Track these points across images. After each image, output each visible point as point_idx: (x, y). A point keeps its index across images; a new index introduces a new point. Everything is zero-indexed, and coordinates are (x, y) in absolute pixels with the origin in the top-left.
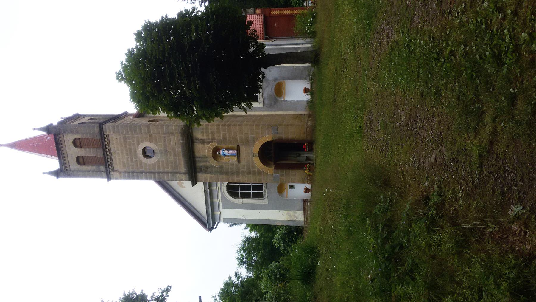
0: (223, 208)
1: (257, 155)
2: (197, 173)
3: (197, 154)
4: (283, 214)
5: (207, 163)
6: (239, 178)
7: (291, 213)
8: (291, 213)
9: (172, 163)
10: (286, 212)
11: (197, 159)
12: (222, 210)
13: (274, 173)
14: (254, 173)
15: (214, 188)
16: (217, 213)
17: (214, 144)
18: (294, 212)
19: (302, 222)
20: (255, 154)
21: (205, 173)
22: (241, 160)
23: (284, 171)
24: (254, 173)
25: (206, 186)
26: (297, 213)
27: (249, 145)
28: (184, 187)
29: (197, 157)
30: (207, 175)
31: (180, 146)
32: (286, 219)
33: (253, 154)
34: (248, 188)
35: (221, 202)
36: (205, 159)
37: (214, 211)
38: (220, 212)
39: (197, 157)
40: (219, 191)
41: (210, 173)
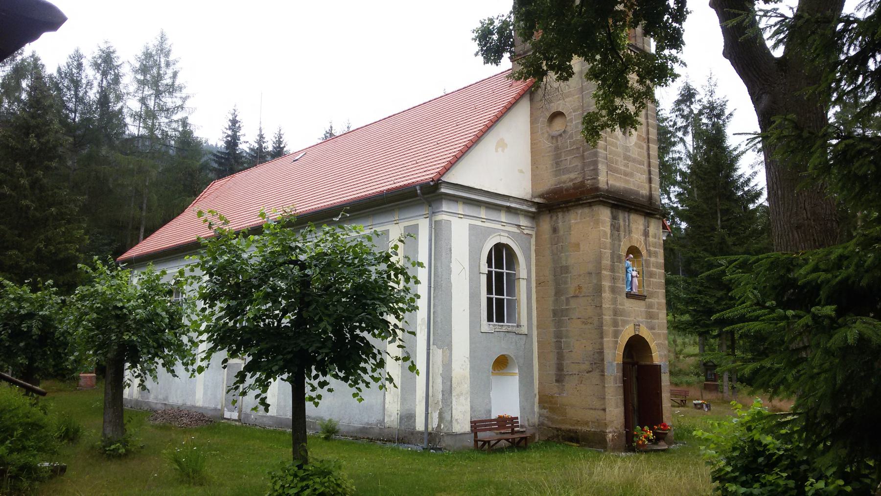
0: (472, 227)
1: (637, 333)
2: (609, 209)
3: (633, 217)
4: (462, 365)
6: (608, 292)
7: (466, 387)
8: (466, 386)
9: (616, 164)
10: (467, 372)
11: (626, 215)
12: (467, 222)
13: (618, 364)
14: (615, 324)
15: (503, 217)
16: (460, 209)
17: (644, 252)
18: (467, 393)
19: (450, 412)
20: (639, 329)
21: (612, 225)
22: (632, 300)
23: (620, 385)
24: (615, 324)
25: (516, 203)
26: (466, 399)
27: (646, 318)
28: (497, 151)
29: (629, 216)
30: (609, 227)
32: (454, 375)
33: (639, 325)
34: (500, 291)
35: (479, 223)
36: (627, 232)
37: (464, 203)
38: (462, 216)
39: (629, 216)
40: (499, 226)
41: (612, 235)
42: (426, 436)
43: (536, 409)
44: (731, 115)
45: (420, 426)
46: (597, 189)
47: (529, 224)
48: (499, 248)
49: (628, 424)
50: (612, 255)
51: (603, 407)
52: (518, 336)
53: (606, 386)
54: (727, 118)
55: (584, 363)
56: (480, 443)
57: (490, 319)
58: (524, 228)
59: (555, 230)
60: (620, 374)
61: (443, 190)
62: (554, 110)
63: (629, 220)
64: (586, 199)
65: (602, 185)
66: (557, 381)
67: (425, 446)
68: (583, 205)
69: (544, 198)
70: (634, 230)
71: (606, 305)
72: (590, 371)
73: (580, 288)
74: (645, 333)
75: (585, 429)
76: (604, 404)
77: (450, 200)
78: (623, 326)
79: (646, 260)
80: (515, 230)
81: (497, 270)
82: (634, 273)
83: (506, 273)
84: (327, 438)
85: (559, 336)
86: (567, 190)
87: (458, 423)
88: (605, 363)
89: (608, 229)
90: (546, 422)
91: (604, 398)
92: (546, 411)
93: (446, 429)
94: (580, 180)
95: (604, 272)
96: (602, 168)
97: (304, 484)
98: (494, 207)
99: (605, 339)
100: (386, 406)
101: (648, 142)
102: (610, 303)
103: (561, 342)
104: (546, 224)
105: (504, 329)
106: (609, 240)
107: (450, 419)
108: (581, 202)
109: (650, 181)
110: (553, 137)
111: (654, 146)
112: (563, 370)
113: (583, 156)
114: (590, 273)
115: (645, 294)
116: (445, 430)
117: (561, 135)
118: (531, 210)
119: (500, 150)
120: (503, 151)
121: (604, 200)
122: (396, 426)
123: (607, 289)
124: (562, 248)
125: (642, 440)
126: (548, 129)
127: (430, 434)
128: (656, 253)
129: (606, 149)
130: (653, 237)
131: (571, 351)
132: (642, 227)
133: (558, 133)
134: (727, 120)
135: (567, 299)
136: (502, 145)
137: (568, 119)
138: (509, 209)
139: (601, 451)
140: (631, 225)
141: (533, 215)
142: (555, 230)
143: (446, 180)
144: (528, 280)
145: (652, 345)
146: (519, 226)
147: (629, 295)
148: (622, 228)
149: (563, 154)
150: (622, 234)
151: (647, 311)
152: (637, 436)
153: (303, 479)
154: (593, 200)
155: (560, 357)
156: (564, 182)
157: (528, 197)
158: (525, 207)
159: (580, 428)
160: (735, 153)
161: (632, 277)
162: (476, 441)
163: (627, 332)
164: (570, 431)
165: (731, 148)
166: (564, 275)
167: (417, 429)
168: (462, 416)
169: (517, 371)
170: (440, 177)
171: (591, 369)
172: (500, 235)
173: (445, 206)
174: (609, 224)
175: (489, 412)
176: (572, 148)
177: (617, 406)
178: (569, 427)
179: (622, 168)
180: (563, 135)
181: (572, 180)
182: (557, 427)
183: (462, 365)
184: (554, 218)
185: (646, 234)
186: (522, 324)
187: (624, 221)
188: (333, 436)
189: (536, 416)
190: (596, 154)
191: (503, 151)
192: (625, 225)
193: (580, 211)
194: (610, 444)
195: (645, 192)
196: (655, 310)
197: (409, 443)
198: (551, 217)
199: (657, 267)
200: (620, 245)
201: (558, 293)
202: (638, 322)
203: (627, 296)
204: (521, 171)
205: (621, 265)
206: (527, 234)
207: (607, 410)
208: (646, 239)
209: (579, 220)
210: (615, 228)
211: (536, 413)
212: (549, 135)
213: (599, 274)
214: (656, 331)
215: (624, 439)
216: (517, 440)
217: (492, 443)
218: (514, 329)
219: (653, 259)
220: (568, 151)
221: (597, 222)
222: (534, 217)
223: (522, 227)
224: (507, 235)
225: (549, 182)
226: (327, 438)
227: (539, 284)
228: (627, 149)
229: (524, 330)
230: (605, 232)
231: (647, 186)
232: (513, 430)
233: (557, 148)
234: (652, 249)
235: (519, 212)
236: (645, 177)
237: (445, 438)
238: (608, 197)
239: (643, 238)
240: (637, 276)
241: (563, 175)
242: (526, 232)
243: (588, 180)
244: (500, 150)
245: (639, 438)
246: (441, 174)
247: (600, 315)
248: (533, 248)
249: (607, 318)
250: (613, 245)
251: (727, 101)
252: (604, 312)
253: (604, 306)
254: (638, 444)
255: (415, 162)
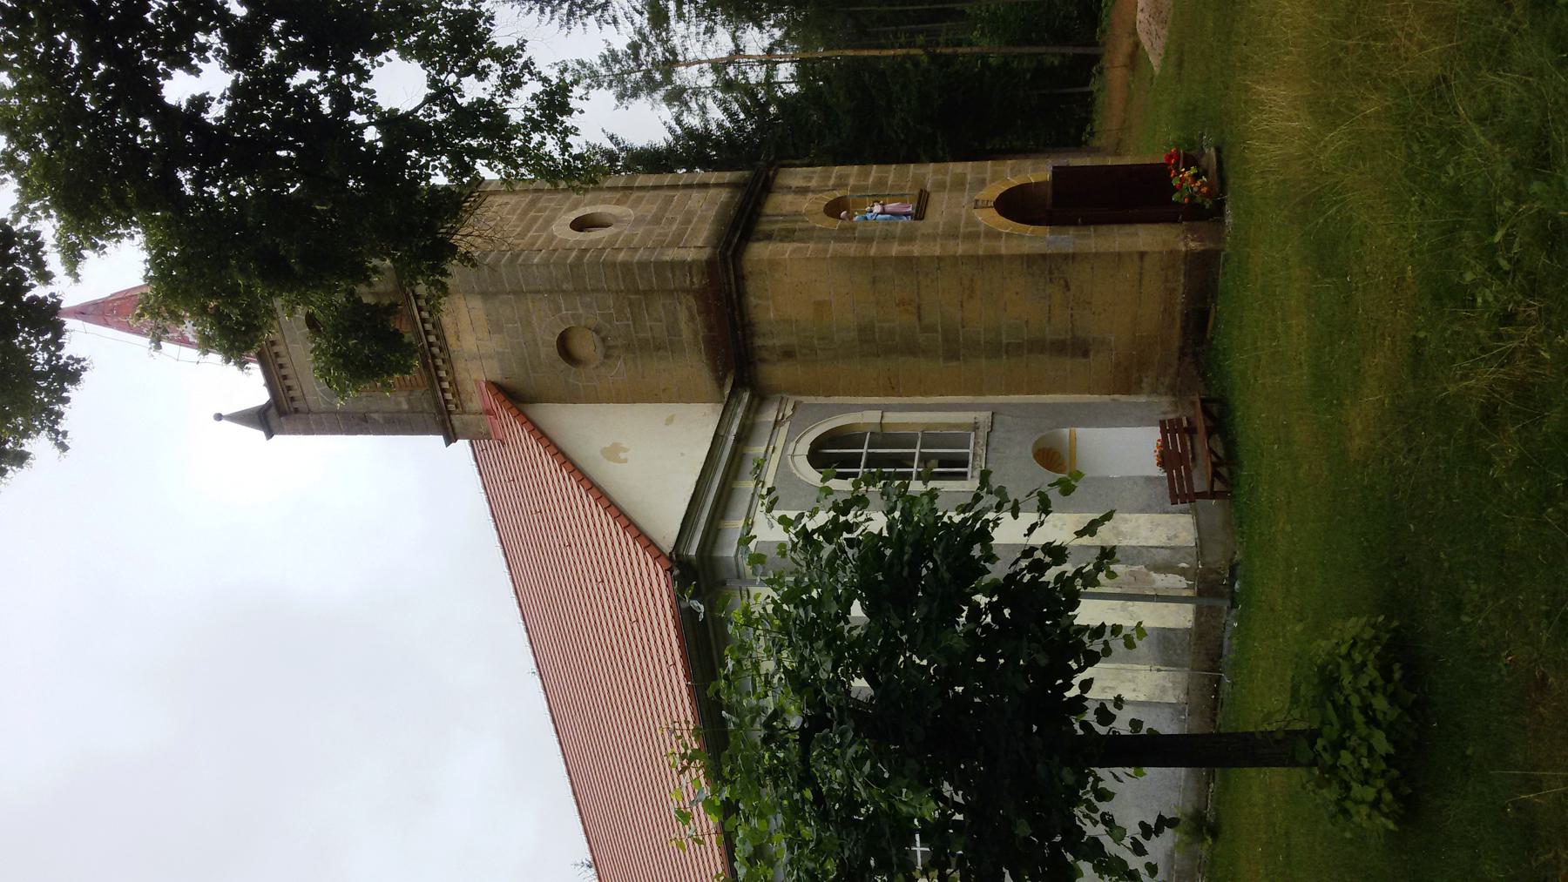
5: (800, 224)
6: (910, 247)
14: (973, 236)
17: (838, 194)
20: (983, 201)
22: (929, 211)
23: (1092, 229)
25: (730, 424)
26: (1126, 521)
27: (964, 190)
28: (625, 461)
30: (786, 245)
31: (716, 207)
33: (977, 201)
37: (723, 517)
40: (775, 459)
41: (801, 240)
42: (1205, 602)
43: (1142, 399)
44: (611, 138)
45: (1180, 617)
46: (710, 263)
47: (776, 406)
48: (817, 457)
49: (1171, 219)
50: (838, 239)
51: (1136, 258)
52: (996, 426)
53: (1094, 250)
54: (617, 144)
55: (1050, 296)
56: (1218, 486)
57: (963, 476)
58: (781, 415)
59: (788, 354)
60: (1072, 231)
61: (693, 552)
62: (554, 351)
63: (774, 216)
64: (729, 284)
65: (705, 254)
66: (1086, 354)
67: (1225, 604)
68: (741, 294)
69: (725, 376)
70: (794, 209)
71: (936, 250)
72: (1066, 282)
73: (902, 303)
74: (993, 192)
75: (1180, 297)
76: (1130, 254)
77: (714, 542)
78: (977, 224)
79: (852, 190)
80: (783, 431)
81: (862, 463)
82: (877, 208)
83: (869, 448)
84: (1214, 832)
85: (996, 349)
86: (710, 328)
87: (1176, 536)
88: (1050, 251)
89: (788, 248)
90: (1167, 381)
91: (1119, 254)
92: (1145, 380)
93: (1190, 559)
94: (692, 302)
95: (872, 252)
96: (670, 255)
97: (1358, 718)
98: (736, 460)
99: (1003, 251)
100: (1142, 698)
101: (631, 188)
102: (932, 244)
103: (1008, 344)
104: (775, 373)
105: (982, 452)
106: (811, 245)
107: (1168, 551)
108: (735, 296)
109: (704, 186)
110: (606, 356)
111: (638, 180)
112: (1063, 343)
113: (645, 292)
114: (874, 282)
115: (916, 192)
116: (1192, 560)
117: (604, 340)
118: (746, 400)
119: (622, 456)
120: (626, 450)
121: (731, 249)
122: (1186, 675)
123: (905, 248)
124: (823, 339)
125: (1200, 188)
126: (592, 366)
127: (1200, 594)
128: (840, 177)
129: (636, 249)
130: (810, 181)
131: (1027, 321)
132: (790, 197)
133: (600, 350)
134: (622, 146)
135: (925, 329)
136: (613, 453)
137: (573, 324)
138: (744, 437)
139: (1226, 256)
140: (784, 212)
141: (756, 401)
142: (788, 354)
143: (672, 545)
144: (886, 408)
145: (1015, 182)
146: (777, 423)
147: (919, 214)
148: (789, 226)
149: (641, 335)
150: (799, 225)
151: (950, 191)
152: (1192, 197)
153: (1348, 725)
154: (732, 272)
155: (1038, 346)
156: (696, 333)
157: (720, 408)
158: (740, 412)
159: (1179, 308)
160: (679, 131)
161: (883, 212)
162: (1213, 495)
163: (990, 218)
164: (1182, 328)
165: (670, 138)
166: (877, 336)
167: (1189, 625)
168: (1160, 528)
169: (1066, 431)
170: (665, 554)
171: (1062, 282)
172: (793, 456)
173: (729, 550)
174: (780, 245)
175: (1149, 480)
176: (629, 315)
177: (1137, 234)
178: (1176, 331)
179: (674, 227)
180: (602, 334)
181: (692, 318)
182: (1177, 355)
183: (1055, 526)
184: (764, 354)
185: (803, 191)
186: (973, 421)
187: (777, 222)
188: (1210, 819)
189: (1155, 399)
190: (643, 265)
191: (626, 450)
192: (783, 221)
193: (753, 300)
194: (1210, 245)
195: (724, 195)
196: (948, 178)
197: (1221, 646)
198: (763, 360)
199: (868, 175)
200: (821, 229)
201: (911, 349)
202: (969, 202)
203: (922, 219)
204: (670, 421)
205: (860, 228)
206: (794, 409)
207: (1143, 249)
208: (813, 191)
209: (770, 302)
210: (788, 235)
211: (1150, 399)
212: (602, 364)
213: (875, 262)
214: (988, 176)
215: (1197, 224)
216: (1209, 423)
217: (1214, 459)
218: (982, 433)
219: (852, 181)
220: (634, 324)
221: (774, 264)
222: (761, 398)
223: (780, 418)
224: (792, 445)
225: (694, 366)
226: (1214, 832)
227: (892, 390)
228: (638, 221)
229: (983, 417)
230: (794, 251)
231: (712, 191)
232: (1186, 430)
233: (628, 348)
234: (832, 182)
235: (748, 422)
236: (696, 195)
237: (1209, 559)
238: (728, 243)
239: (810, 196)
240: (883, 205)
241: (681, 336)
242: (789, 412)
243: (692, 282)
244: (622, 456)
245: (1196, 193)
246: (658, 554)
247: (956, 260)
248: (821, 400)
249: (961, 248)
250: (820, 239)
251: (587, 143)
252: (951, 253)
253: (937, 253)
254: (1208, 195)
255: (635, 625)
